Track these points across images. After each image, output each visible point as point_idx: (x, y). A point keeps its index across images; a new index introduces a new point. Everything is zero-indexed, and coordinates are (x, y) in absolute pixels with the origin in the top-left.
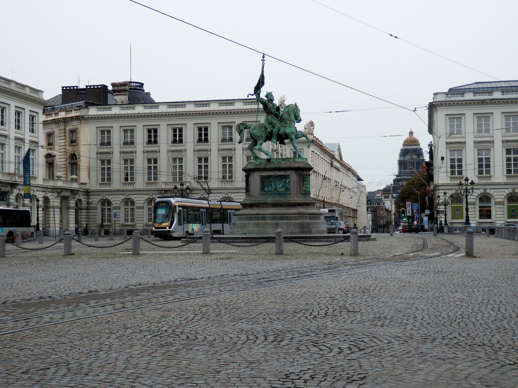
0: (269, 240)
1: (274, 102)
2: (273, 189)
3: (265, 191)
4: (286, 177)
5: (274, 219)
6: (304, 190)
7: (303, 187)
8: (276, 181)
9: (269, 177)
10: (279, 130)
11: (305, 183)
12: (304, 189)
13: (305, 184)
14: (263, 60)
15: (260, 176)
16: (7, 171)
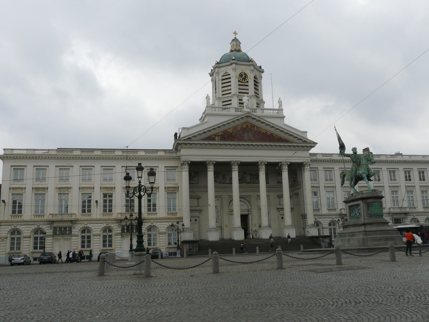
0: (385, 250)
1: (358, 153)
2: (354, 214)
3: (351, 217)
4: (358, 205)
5: (349, 236)
6: (369, 214)
7: (368, 211)
8: (355, 209)
9: (352, 206)
10: (356, 172)
11: (370, 208)
12: (369, 212)
13: (370, 209)
14: (336, 130)
15: (348, 206)
16: (400, 206)
